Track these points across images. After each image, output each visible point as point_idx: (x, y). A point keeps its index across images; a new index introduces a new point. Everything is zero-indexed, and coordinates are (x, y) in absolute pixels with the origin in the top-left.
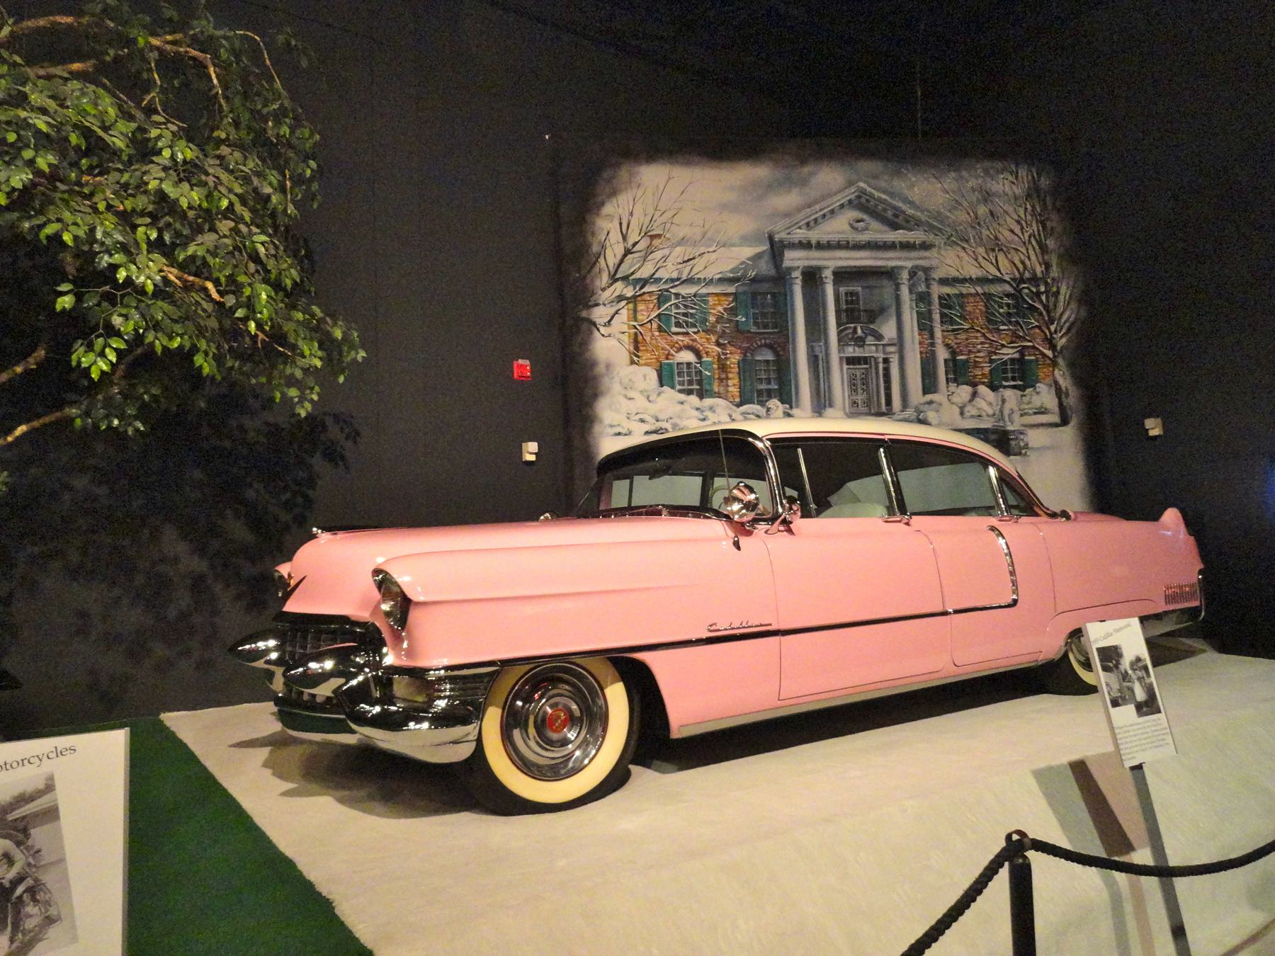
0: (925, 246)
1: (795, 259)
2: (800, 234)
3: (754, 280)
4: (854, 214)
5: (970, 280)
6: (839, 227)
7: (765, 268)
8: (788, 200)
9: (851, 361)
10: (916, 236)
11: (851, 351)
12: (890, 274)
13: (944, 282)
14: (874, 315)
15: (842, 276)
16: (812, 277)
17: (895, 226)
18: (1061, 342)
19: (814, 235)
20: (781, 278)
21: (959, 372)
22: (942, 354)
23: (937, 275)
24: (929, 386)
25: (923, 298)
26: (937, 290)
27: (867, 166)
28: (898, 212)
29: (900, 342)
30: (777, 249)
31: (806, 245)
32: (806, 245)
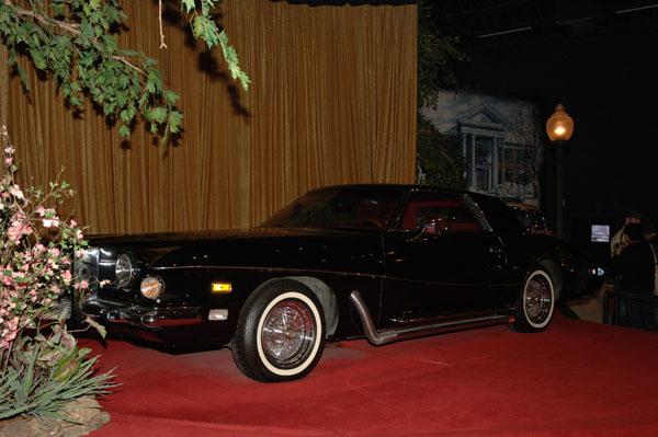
0: (502, 130)
1: (464, 130)
2: (466, 121)
3: (451, 137)
4: (482, 116)
5: (514, 144)
6: (477, 120)
7: (455, 132)
8: (464, 107)
9: (479, 170)
10: (499, 126)
11: (478, 166)
12: (491, 139)
13: (507, 144)
14: (486, 154)
15: (478, 138)
16: (469, 137)
17: (493, 121)
18: (537, 169)
19: (470, 122)
20: (460, 135)
21: (509, 178)
22: (504, 170)
23: (505, 141)
24: (500, 182)
25: (500, 149)
26: (505, 147)
27: (487, 98)
28: (495, 116)
29: (492, 165)
30: (459, 125)
31: (468, 125)
32: (468, 125)
